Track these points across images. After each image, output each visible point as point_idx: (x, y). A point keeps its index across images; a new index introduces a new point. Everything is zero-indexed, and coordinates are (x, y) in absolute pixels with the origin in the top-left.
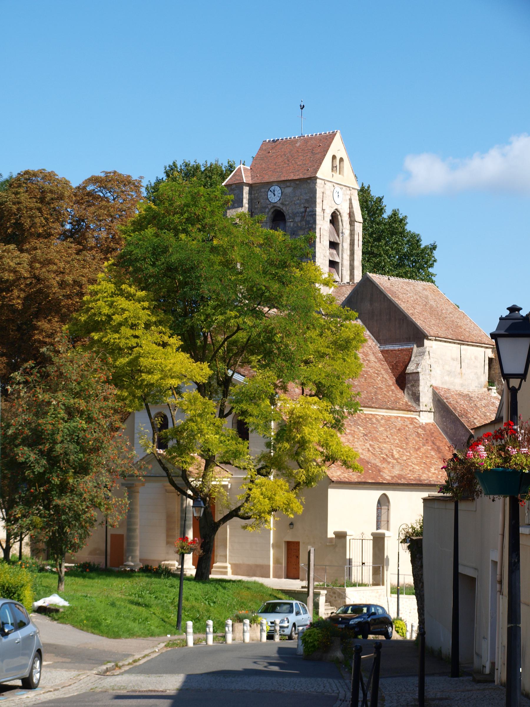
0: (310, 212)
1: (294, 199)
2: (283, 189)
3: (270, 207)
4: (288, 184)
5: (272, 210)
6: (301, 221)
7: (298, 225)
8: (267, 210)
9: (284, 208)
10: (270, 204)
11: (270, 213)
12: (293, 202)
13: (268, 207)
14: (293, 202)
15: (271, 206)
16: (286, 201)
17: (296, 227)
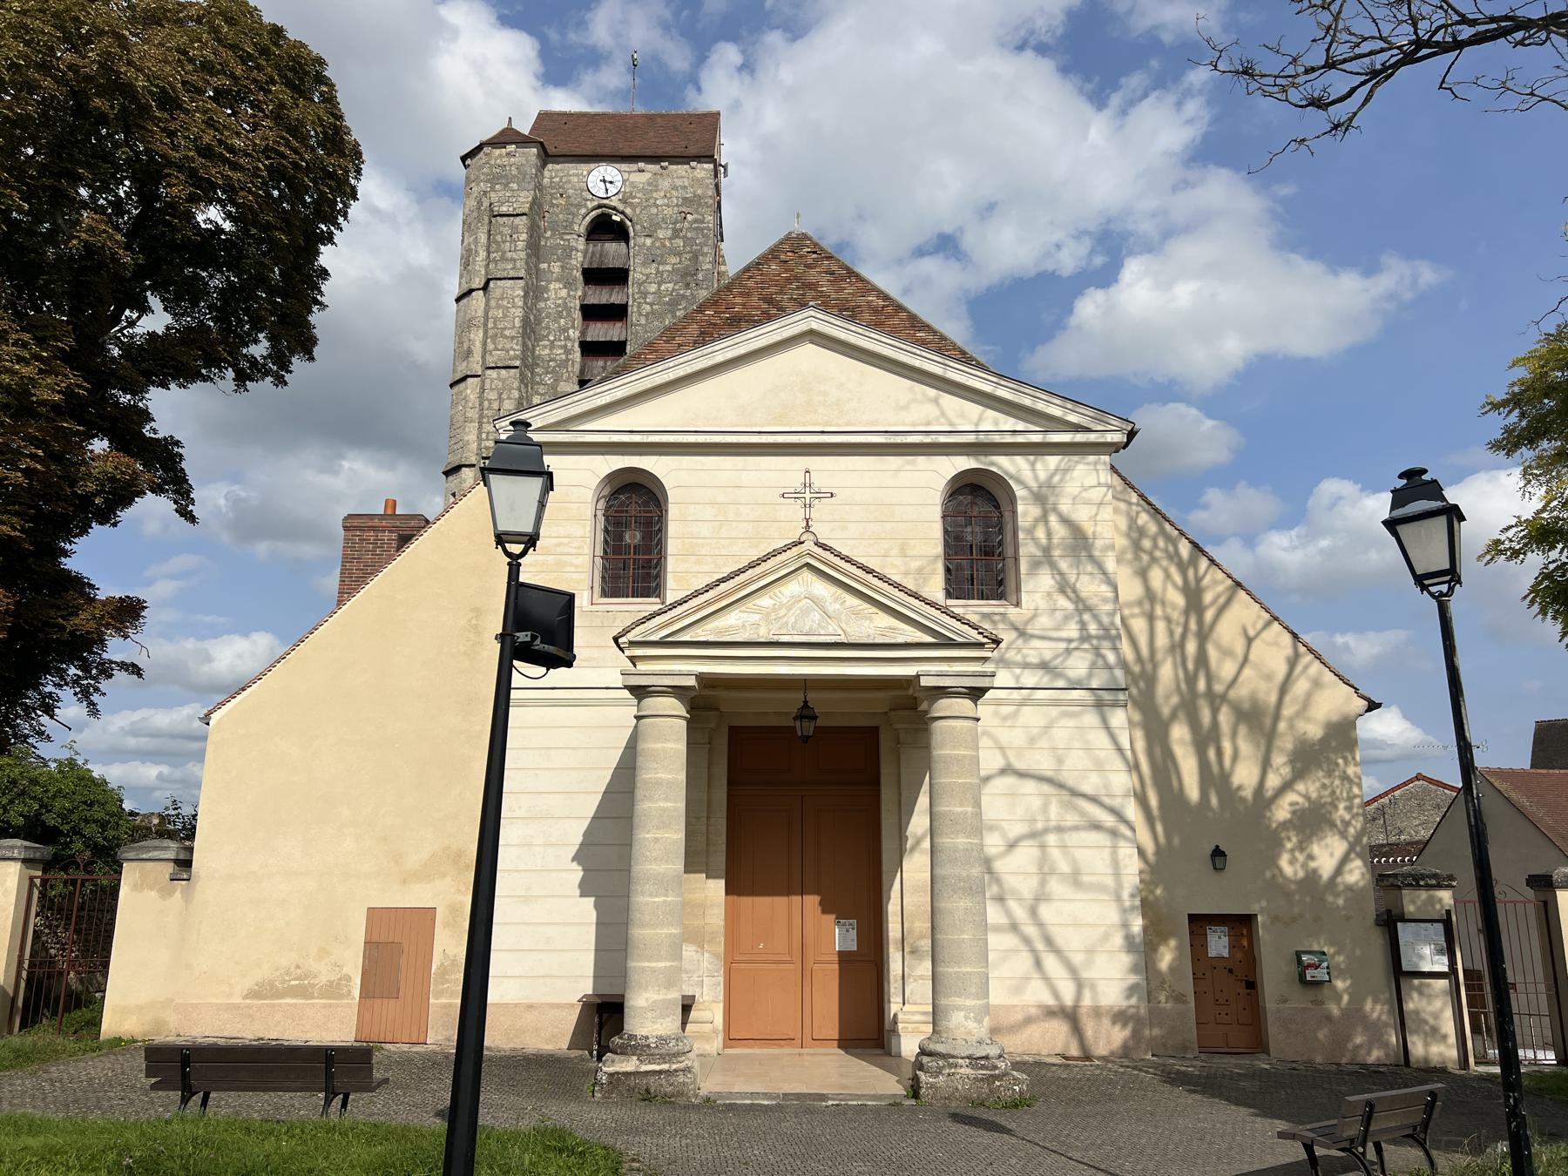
0: (696, 221)
1: (655, 195)
2: (626, 176)
3: (590, 205)
4: (641, 165)
5: (594, 213)
6: (670, 239)
7: (664, 246)
8: (583, 211)
9: (628, 211)
10: (592, 200)
11: (588, 219)
12: (652, 201)
13: (585, 206)
14: (652, 201)
15: (596, 203)
16: (635, 197)
17: (658, 248)
